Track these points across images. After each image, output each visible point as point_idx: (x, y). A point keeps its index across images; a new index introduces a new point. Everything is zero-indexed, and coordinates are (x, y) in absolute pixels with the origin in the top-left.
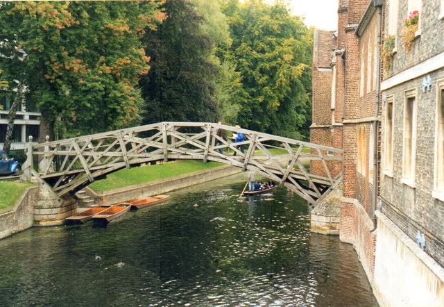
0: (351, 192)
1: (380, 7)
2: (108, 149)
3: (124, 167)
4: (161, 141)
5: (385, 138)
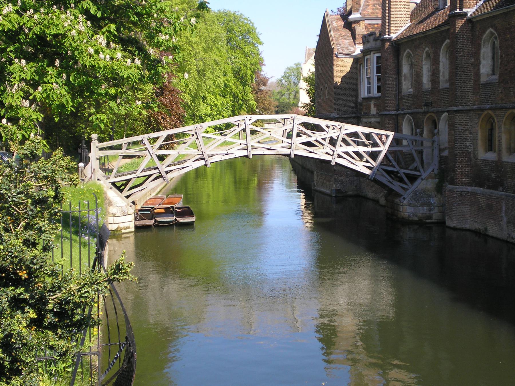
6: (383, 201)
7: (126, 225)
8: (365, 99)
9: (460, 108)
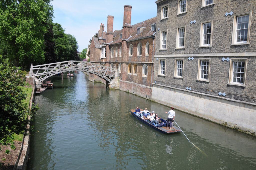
0: (124, 79)
6: (105, 84)
8: (102, 58)
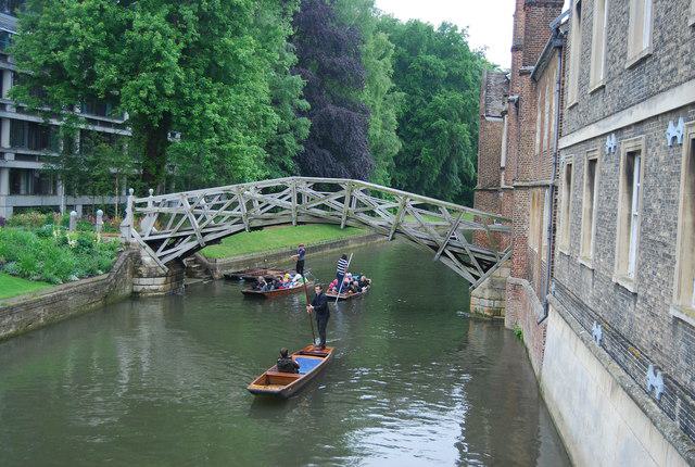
0: (520, 271)
1: (560, 48)
2: (224, 207)
3: (244, 230)
4: (289, 200)
5: (562, 206)
7: (154, 287)
9: (520, 184)
